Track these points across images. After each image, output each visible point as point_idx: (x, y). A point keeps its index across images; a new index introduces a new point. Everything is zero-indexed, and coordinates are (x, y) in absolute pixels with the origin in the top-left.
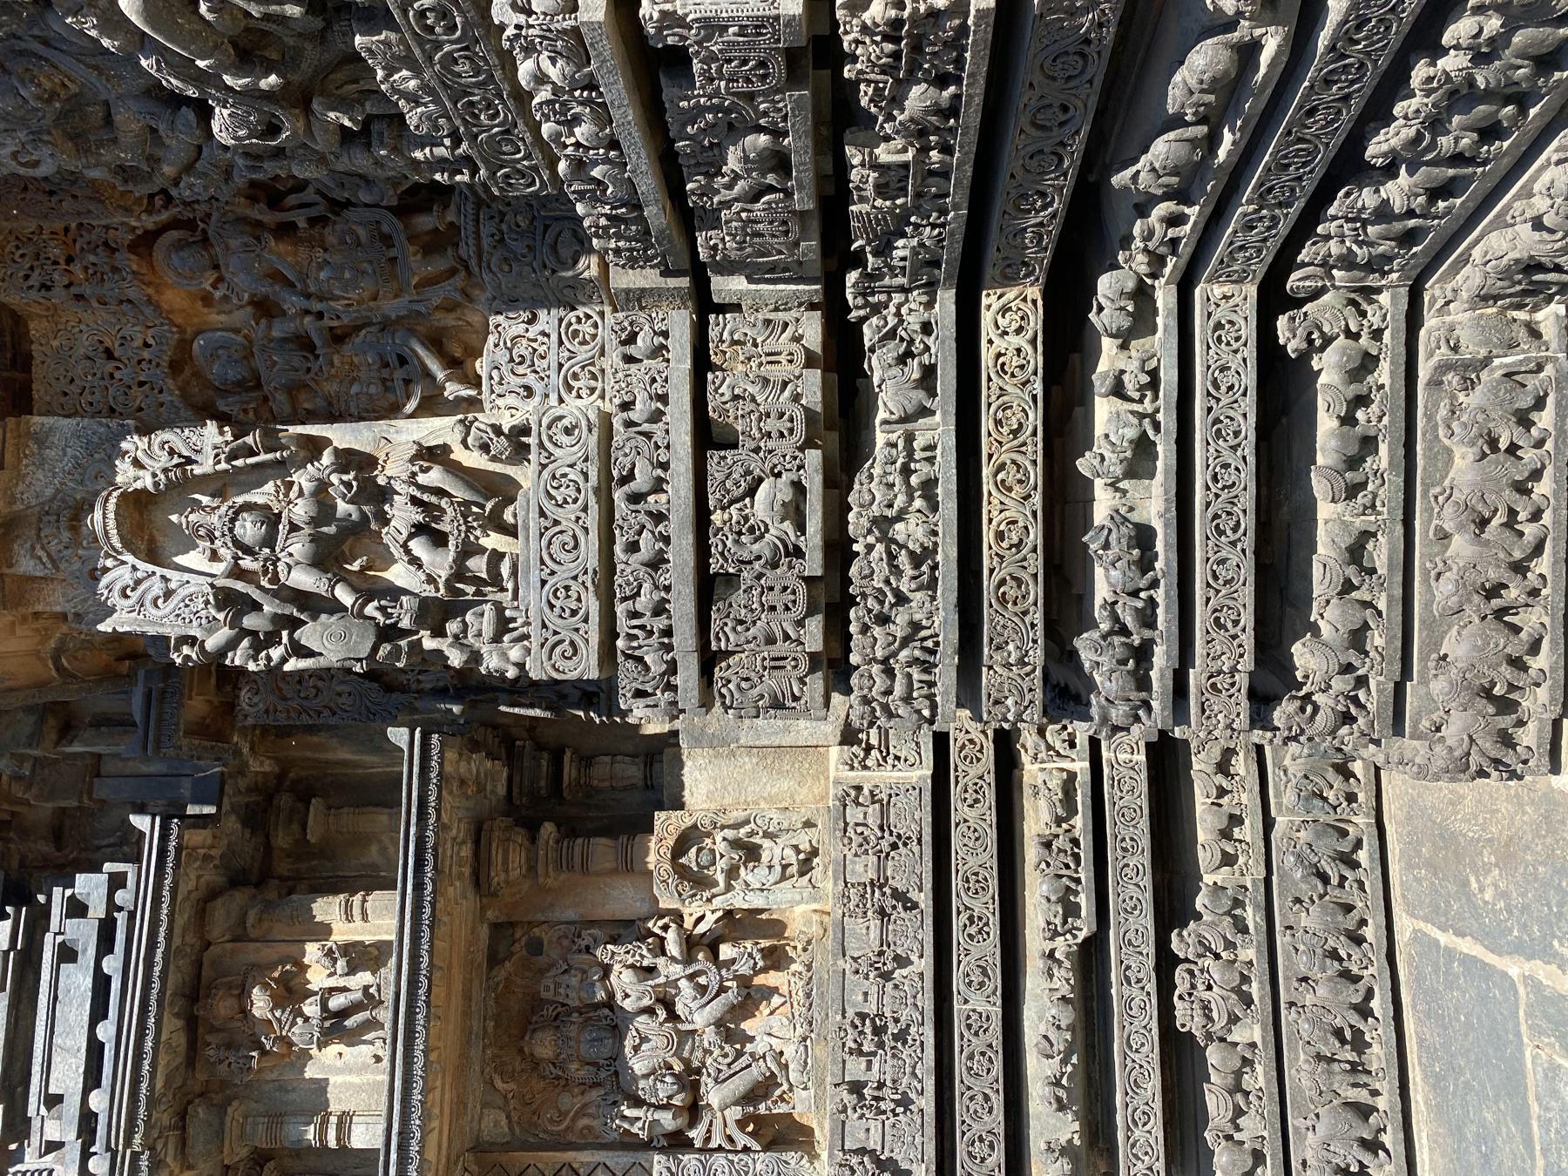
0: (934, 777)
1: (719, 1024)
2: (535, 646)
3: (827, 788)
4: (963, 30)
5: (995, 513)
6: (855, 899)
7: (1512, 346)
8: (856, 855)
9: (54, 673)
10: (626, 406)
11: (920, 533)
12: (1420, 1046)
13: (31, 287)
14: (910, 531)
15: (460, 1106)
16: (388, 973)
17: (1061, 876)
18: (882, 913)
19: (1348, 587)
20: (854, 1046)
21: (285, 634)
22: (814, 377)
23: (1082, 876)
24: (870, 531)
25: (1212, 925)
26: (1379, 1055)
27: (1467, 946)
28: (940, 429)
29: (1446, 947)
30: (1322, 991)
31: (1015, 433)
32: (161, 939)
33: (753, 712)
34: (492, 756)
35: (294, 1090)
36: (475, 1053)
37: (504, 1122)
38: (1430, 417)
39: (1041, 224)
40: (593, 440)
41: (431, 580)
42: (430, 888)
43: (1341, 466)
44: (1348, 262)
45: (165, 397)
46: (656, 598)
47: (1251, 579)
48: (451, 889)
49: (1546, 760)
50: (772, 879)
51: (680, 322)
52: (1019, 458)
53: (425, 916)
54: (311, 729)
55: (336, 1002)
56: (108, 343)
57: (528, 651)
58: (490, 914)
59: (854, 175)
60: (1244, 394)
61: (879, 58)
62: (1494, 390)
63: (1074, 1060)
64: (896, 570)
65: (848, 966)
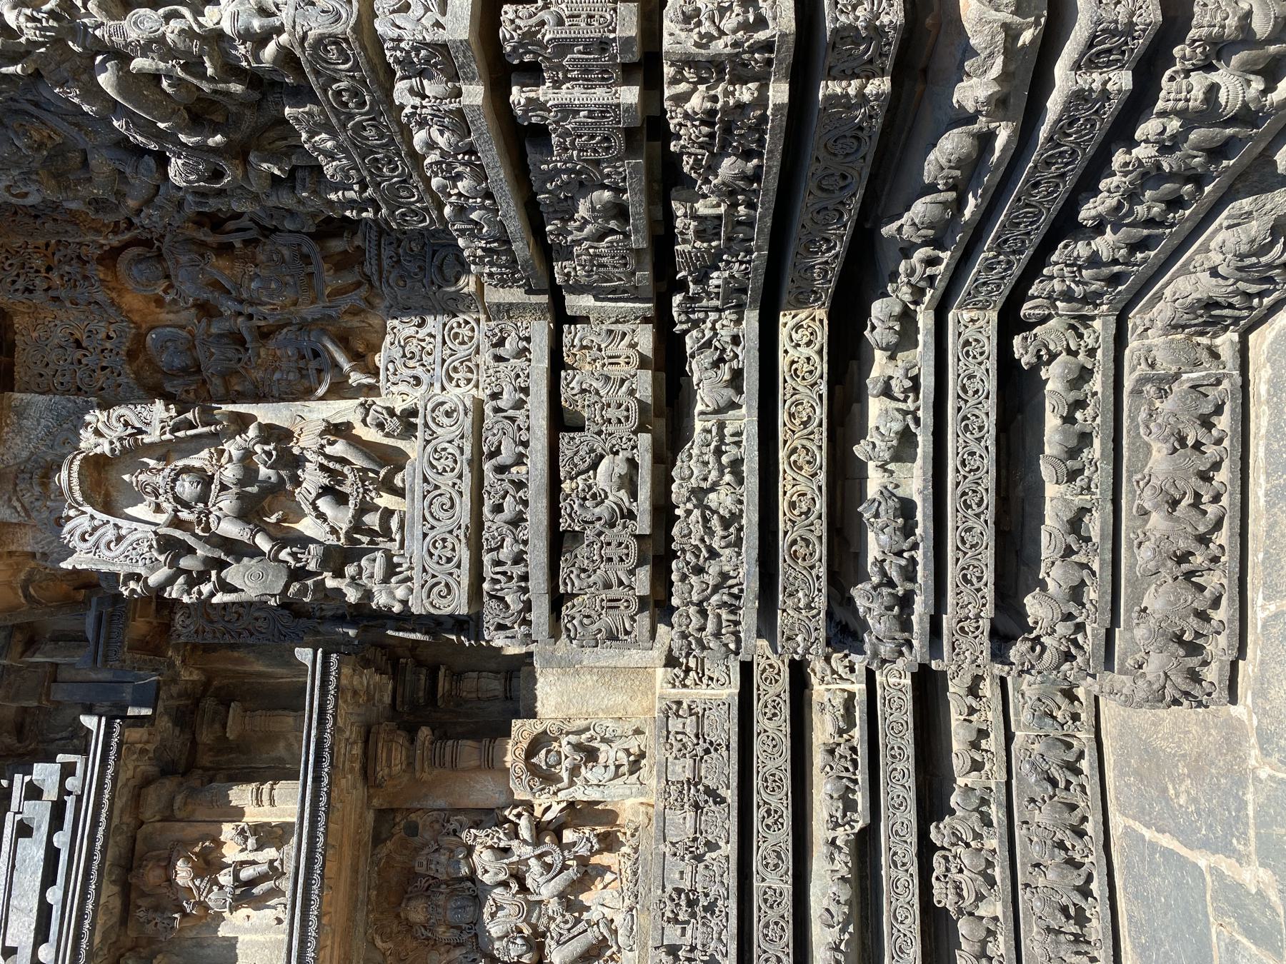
0: (741, 695)
1: (561, 896)
2: (416, 586)
3: (654, 702)
4: (763, 119)
5: (789, 487)
6: (674, 795)
7: (1196, 364)
8: (676, 758)
9: (23, 600)
10: (495, 396)
12: (1130, 922)
13: (17, 290)
14: (721, 500)
16: (290, 849)
17: (842, 778)
18: (696, 806)
19: (1069, 552)
20: (671, 915)
21: (214, 573)
22: (646, 376)
23: (859, 778)
24: (689, 499)
25: (963, 819)
26: (1097, 928)
27: (1166, 841)
28: (745, 419)
29: (1150, 842)
30: (1051, 875)
31: (805, 424)
32: (103, 819)
33: (593, 643)
34: (380, 671)
35: (209, 946)
36: (360, 916)
38: (1133, 419)
39: (826, 263)
40: (469, 421)
41: (334, 531)
42: (326, 781)
43: (1063, 456)
44: (1068, 296)
45: (122, 380)
46: (516, 549)
47: (992, 544)
48: (344, 781)
49: (1225, 693)
50: (607, 776)
51: (540, 331)
53: (322, 804)
54: (232, 647)
55: (246, 874)
56: (78, 335)
57: (411, 590)
58: (375, 802)
59: (679, 223)
60: (987, 397)
61: (698, 137)
62: (1183, 398)
63: (851, 929)
64: (710, 531)
65: (668, 850)
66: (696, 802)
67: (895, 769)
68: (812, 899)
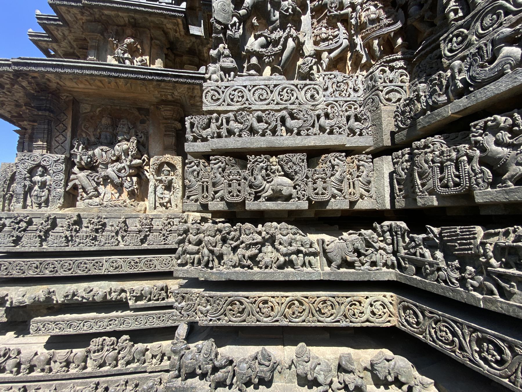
2: (219, 83)
5: (277, 300)
11: (267, 259)
15: (88, 95)
17: (151, 294)
18: (140, 231)
22: (345, 206)
24: (268, 233)
25: (130, 351)
32: (147, 9)
37: (86, 111)
42: (150, 78)
53: (140, 76)
57: (217, 81)
64: (248, 247)
65: (122, 220)
66: (142, 231)
67: (154, 318)
68: (99, 282)
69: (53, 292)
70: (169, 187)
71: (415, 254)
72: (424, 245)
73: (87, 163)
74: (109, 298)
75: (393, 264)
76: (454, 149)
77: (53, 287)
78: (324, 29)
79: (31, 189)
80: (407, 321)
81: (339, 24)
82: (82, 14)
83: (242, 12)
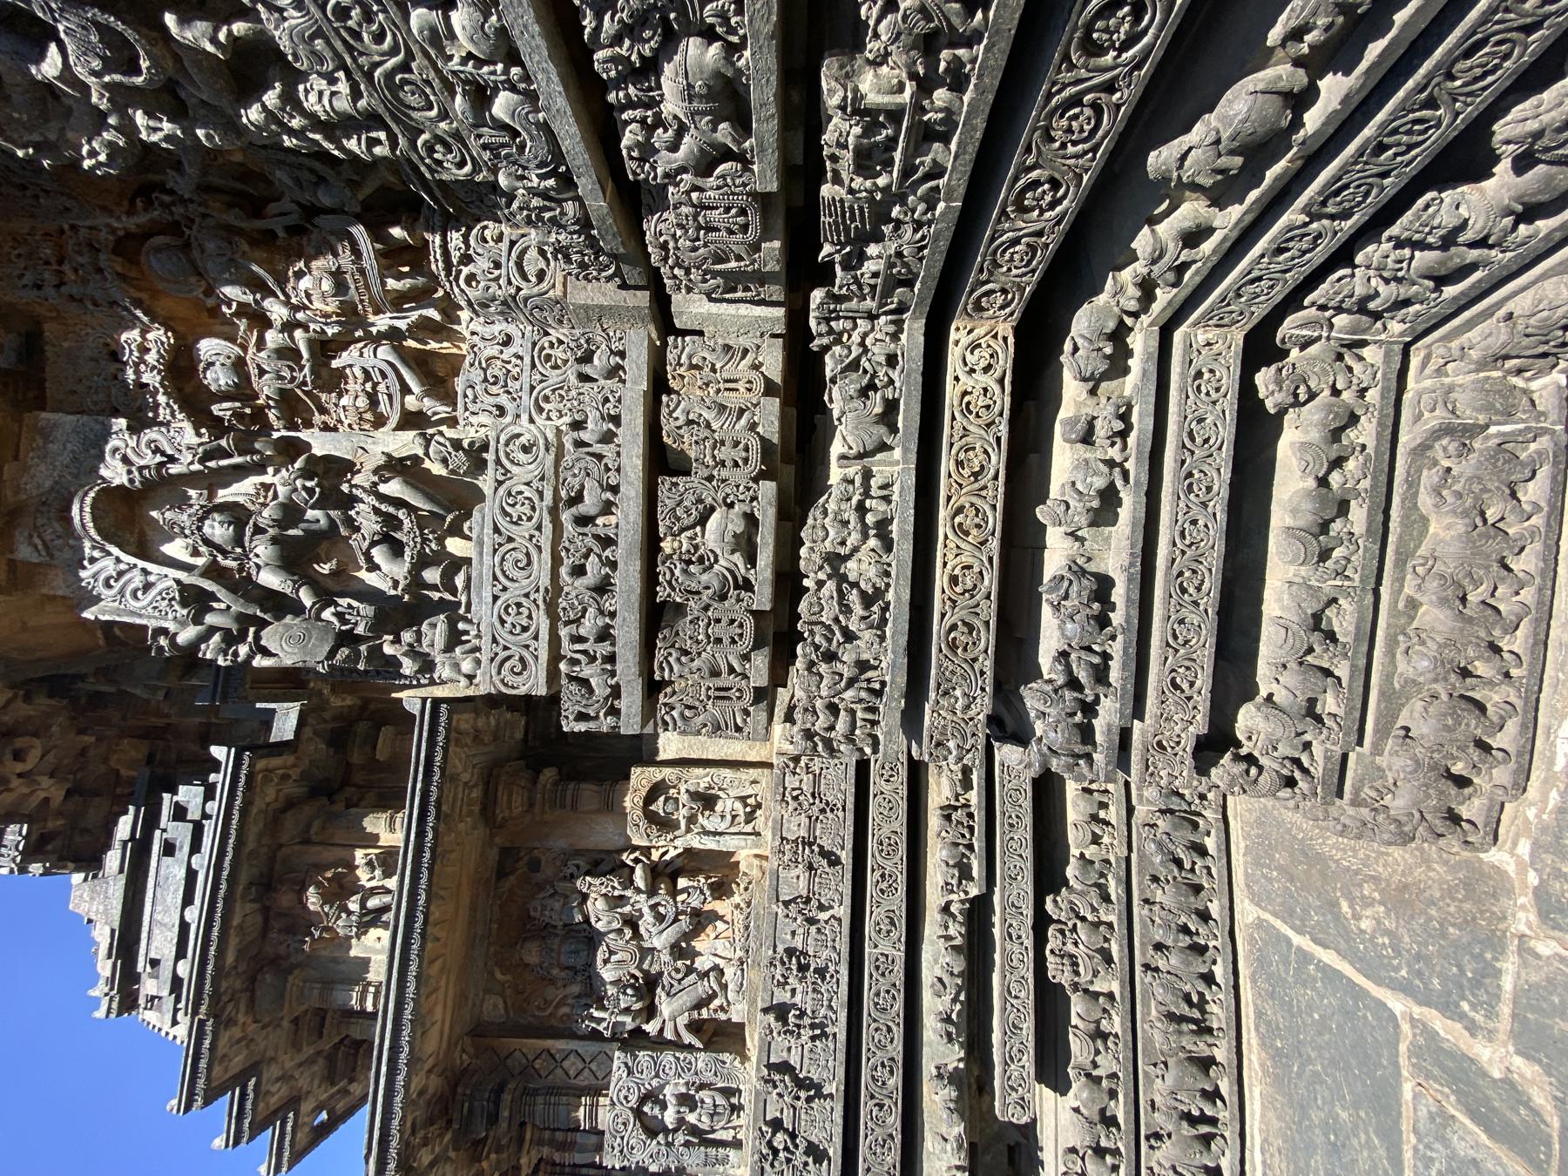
2: (484, 657)
5: (950, 556)
9: (101, 642)
10: (577, 425)
11: (872, 572)
13: (25, 286)
15: (461, 999)
17: (957, 845)
18: (810, 867)
21: (252, 630)
22: (774, 404)
24: (821, 568)
25: (1082, 894)
29: (1299, 949)
31: (976, 475)
32: (230, 849)
39: (1040, 234)
40: (551, 458)
42: (430, 836)
43: (1316, 530)
44: (1362, 307)
46: (600, 623)
47: (1211, 642)
51: (638, 341)
52: (978, 502)
55: (373, 903)
57: (478, 662)
60: (1220, 448)
64: (846, 609)
65: (781, 910)
68: (924, 965)
69: (938, 1068)
70: (707, 801)
71: (873, 287)
72: (855, 268)
73: (639, 994)
74: (958, 941)
75: (892, 322)
76: (675, 208)
77: (928, 1069)
78: (344, 401)
79: (694, 1130)
80: (1002, 308)
81: (335, 364)
82: (230, 1022)
83: (306, 597)
